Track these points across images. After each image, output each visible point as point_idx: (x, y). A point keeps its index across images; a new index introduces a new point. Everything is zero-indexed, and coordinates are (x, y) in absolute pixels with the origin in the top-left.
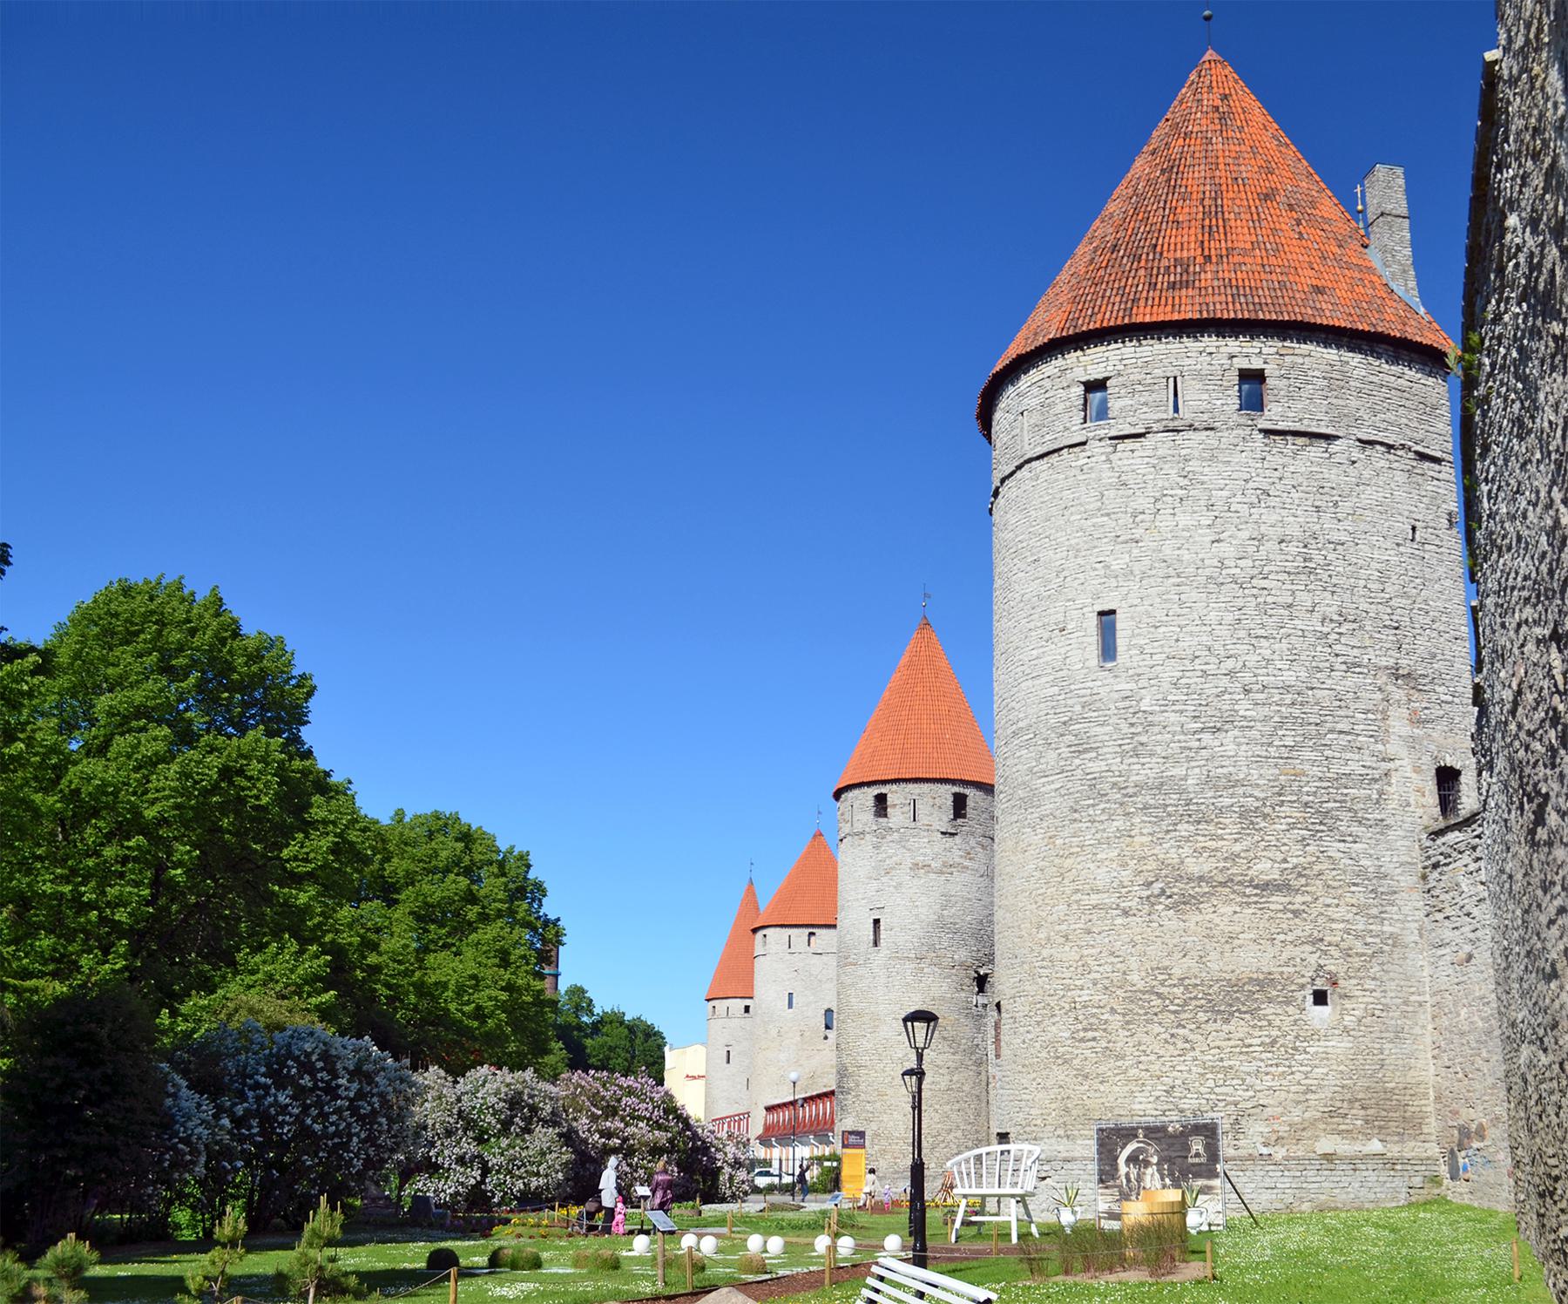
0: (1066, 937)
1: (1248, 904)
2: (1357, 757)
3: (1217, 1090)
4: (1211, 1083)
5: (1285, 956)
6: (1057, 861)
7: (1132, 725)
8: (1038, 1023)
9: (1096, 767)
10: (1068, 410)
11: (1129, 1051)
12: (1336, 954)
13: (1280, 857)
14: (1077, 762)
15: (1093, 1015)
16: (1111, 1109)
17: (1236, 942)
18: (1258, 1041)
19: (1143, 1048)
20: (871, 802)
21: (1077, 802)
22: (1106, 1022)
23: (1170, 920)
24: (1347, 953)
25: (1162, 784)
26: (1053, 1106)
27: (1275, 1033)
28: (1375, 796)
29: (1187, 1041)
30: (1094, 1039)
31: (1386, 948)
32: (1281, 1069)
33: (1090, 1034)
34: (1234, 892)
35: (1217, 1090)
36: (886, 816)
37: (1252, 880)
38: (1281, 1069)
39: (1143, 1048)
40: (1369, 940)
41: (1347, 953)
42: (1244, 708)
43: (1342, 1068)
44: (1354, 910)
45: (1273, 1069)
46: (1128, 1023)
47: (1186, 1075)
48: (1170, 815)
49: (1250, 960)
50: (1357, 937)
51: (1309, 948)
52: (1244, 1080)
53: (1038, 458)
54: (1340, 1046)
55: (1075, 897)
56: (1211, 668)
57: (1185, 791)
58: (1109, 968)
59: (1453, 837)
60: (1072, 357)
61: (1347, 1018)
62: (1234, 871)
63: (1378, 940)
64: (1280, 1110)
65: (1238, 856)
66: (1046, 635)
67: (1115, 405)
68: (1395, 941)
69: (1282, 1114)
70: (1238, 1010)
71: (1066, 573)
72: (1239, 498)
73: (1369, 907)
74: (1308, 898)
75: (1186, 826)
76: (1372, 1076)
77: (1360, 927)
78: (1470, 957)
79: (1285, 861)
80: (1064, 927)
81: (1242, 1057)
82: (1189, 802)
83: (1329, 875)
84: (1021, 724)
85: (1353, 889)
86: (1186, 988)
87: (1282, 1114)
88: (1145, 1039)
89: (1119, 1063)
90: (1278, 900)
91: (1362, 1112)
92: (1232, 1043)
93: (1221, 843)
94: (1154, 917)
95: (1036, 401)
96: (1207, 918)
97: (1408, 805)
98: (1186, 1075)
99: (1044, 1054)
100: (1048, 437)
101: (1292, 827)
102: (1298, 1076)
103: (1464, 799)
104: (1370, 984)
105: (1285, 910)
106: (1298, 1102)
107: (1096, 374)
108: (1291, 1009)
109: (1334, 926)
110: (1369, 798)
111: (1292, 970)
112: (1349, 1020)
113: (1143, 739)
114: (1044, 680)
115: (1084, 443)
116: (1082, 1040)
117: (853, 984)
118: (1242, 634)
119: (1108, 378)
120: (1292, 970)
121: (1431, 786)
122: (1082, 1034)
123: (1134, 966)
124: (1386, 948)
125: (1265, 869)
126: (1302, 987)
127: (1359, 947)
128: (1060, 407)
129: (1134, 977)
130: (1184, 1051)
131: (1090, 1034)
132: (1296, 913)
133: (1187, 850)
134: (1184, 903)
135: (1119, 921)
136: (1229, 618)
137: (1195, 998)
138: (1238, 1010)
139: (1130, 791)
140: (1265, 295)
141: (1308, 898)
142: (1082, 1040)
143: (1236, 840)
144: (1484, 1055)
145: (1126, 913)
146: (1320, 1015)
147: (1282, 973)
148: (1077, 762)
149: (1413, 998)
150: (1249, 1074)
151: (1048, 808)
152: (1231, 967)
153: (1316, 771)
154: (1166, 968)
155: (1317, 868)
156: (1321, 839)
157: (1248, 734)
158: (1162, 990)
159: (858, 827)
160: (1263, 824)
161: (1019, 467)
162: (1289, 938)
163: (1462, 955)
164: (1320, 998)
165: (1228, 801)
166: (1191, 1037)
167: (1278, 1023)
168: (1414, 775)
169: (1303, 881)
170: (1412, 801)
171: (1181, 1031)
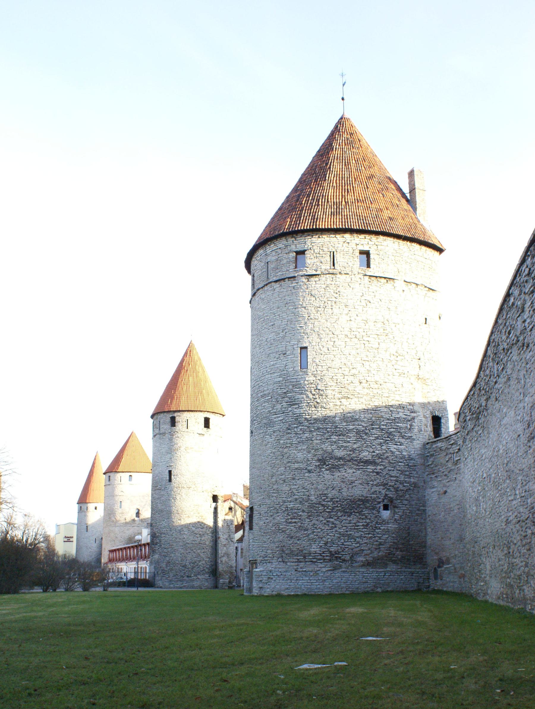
0: (284, 481)
1: (359, 469)
2: (403, 411)
3: (345, 543)
4: (342, 541)
5: (373, 490)
6: (281, 449)
7: (314, 395)
8: (271, 516)
9: (297, 411)
10: (288, 262)
11: (309, 527)
12: (393, 490)
13: (372, 450)
14: (290, 409)
15: (295, 513)
16: (302, 551)
17: (354, 484)
18: (361, 524)
19: (315, 526)
20: (168, 420)
21: (290, 426)
22: (301, 515)
23: (327, 475)
24: (397, 490)
25: (326, 419)
27: (368, 521)
28: (409, 427)
29: (333, 524)
30: (295, 522)
31: (412, 488)
32: (370, 535)
33: (294, 520)
34: (353, 464)
35: (345, 543)
36: (175, 426)
37: (361, 459)
38: (370, 535)
39: (315, 526)
40: (405, 484)
41: (397, 490)
42: (359, 388)
43: (394, 535)
44: (400, 472)
45: (367, 535)
46: (309, 516)
47: (333, 537)
48: (328, 432)
49: (359, 491)
50: (400, 483)
51: (382, 487)
52: (355, 540)
53: (276, 281)
54: (392, 526)
55: (289, 464)
56: (346, 373)
57: (335, 423)
58: (302, 494)
59: (439, 444)
60: (290, 240)
61: (396, 515)
62: (354, 455)
63: (408, 485)
64: (369, 552)
65: (355, 449)
66: (277, 356)
67: (308, 261)
68: (415, 485)
69: (370, 554)
70: (354, 512)
71: (287, 331)
72: (359, 303)
73: (406, 471)
74: (382, 467)
75: (335, 437)
76: (405, 538)
77: (402, 479)
78: (445, 492)
79: (374, 452)
80: (283, 477)
81: (355, 531)
82: (336, 427)
83: (391, 458)
84: (265, 393)
85: (400, 464)
86: (333, 503)
87: (370, 554)
88: (317, 522)
89: (306, 532)
90: (371, 468)
91: (401, 553)
92: (351, 525)
93: (349, 444)
94: (321, 473)
95: (274, 258)
96: (343, 474)
97: (421, 431)
98: (333, 537)
99: (274, 528)
100: (279, 273)
101: (377, 438)
102: (377, 538)
103: (442, 429)
104: (406, 502)
105: (373, 472)
106: (376, 549)
107: (300, 248)
108: (374, 512)
109: (392, 478)
110: (407, 427)
111: (375, 496)
112: (397, 517)
113: (319, 401)
114: (276, 374)
115: (295, 277)
116: (291, 523)
117: (158, 498)
118: (358, 359)
119: (306, 250)
120: (375, 496)
121: (430, 422)
122: (290, 520)
123: (313, 493)
124: (412, 488)
125: (365, 455)
126: (379, 503)
127: (401, 487)
128: (285, 261)
129: (312, 498)
130: (332, 528)
131: (294, 520)
132: (378, 473)
133: (334, 447)
134: (333, 468)
135: (307, 475)
136: (354, 352)
137: (337, 506)
138: (354, 512)
139: (312, 422)
140: (370, 220)
141: (382, 467)
142: (291, 523)
143: (355, 443)
144: (451, 531)
145: (309, 472)
146: (386, 514)
147: (371, 497)
148: (290, 409)
149: (421, 508)
150: (357, 537)
151: (277, 427)
152: (351, 494)
153: (387, 416)
154: (325, 494)
155: (386, 455)
156: (388, 443)
157: (361, 400)
158: (324, 503)
159: (162, 431)
160: (365, 437)
161: (267, 285)
162: (375, 483)
163: (442, 491)
164: (386, 508)
165: (351, 427)
166: (335, 522)
167: (369, 517)
168: (423, 419)
169: (380, 460)
170: (423, 430)
171: (331, 520)
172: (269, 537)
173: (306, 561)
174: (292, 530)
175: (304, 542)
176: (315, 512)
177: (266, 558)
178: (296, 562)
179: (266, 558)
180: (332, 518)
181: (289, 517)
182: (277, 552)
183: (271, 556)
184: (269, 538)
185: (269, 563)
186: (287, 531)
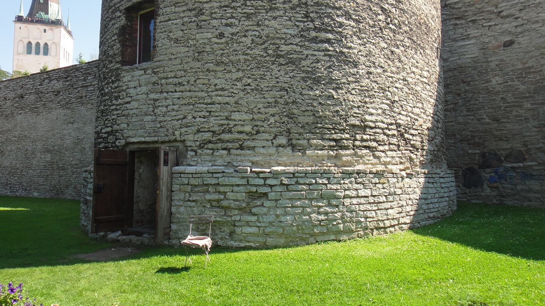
8: (248, 16)
22: (341, 25)
26: (272, 110)
116: (315, 40)
122: (313, 34)
142: (315, 40)
172: (240, 74)
173: (358, 147)
174: (318, 61)
175: (351, 97)
176: (371, 23)
177: (226, 136)
178: (331, 148)
179: (226, 136)
180: (398, 48)
181: (311, 25)
182: (272, 120)
183: (248, 129)
184: (239, 79)
185: (241, 148)
186: (304, 63)
